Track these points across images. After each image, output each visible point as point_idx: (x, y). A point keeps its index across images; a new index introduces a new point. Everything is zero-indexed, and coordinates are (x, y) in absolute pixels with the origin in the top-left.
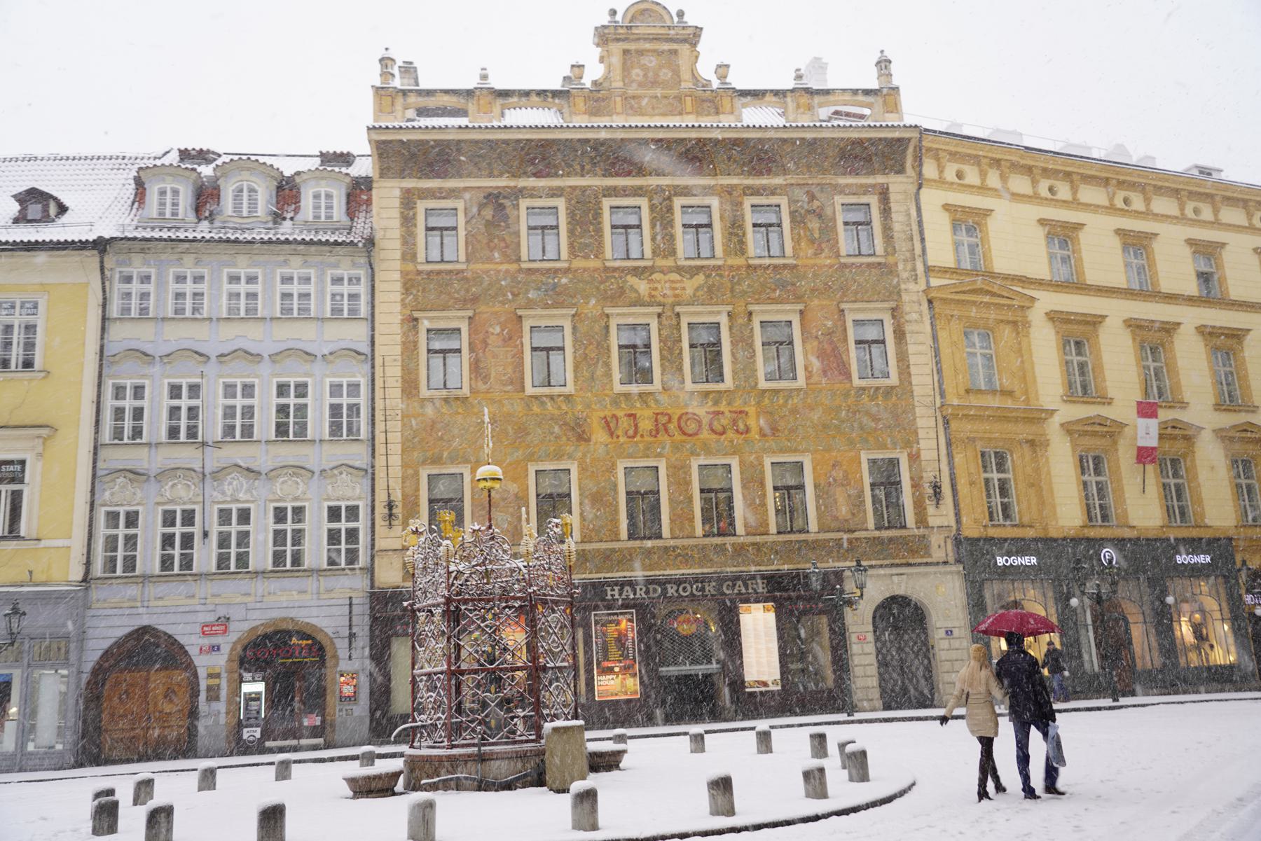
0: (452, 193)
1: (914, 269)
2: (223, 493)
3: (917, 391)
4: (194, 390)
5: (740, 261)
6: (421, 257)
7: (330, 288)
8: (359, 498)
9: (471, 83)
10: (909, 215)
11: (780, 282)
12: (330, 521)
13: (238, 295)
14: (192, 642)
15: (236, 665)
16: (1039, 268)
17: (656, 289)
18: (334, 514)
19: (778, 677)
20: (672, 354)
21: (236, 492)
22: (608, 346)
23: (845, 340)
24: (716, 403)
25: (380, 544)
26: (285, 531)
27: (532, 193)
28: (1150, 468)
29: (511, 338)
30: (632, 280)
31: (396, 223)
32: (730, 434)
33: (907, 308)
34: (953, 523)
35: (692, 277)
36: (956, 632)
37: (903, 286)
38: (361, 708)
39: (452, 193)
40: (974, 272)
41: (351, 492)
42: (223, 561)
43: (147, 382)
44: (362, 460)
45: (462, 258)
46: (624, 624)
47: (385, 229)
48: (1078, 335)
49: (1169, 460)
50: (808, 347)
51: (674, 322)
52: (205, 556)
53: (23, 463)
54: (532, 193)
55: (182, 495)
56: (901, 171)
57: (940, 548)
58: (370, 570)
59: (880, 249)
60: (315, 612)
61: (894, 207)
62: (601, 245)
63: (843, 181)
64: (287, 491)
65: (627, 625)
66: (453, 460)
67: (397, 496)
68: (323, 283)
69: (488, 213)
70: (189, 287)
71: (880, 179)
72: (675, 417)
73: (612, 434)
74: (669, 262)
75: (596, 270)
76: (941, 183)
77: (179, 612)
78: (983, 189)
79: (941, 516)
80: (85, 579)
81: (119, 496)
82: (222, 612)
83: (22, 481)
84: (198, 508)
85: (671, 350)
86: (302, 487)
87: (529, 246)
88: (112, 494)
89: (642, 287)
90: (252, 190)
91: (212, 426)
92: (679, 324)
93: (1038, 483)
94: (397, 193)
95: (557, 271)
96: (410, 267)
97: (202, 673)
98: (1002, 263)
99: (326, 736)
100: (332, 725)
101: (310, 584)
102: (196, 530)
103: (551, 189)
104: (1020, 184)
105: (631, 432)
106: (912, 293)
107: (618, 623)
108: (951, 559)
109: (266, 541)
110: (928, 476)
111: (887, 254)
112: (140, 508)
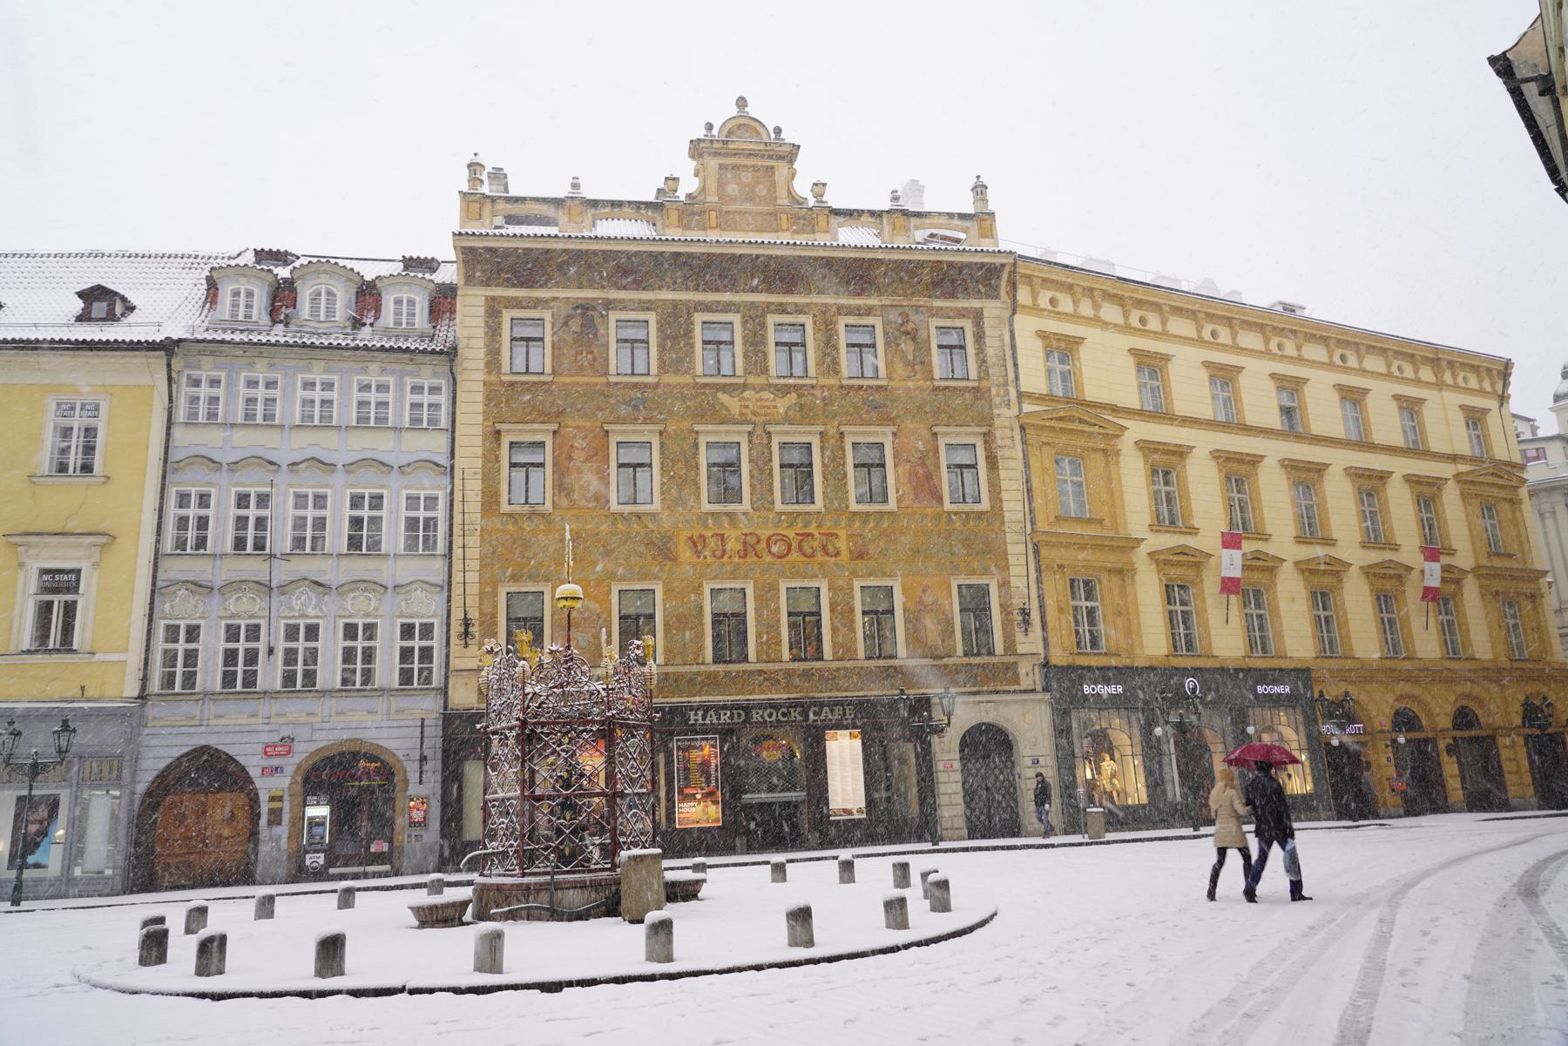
0: (537, 303)
1: (1008, 394)
2: (291, 609)
3: (1008, 516)
4: (263, 500)
5: (832, 381)
6: (506, 368)
7: (410, 398)
8: (434, 616)
9: (562, 191)
10: (1002, 341)
11: (875, 404)
12: (402, 638)
13: (313, 402)
14: (253, 764)
15: (299, 788)
16: (1129, 397)
18: (407, 631)
19: (863, 804)
21: (304, 606)
23: (938, 466)
24: (806, 525)
25: (456, 663)
26: (354, 648)
27: (622, 305)
28: (1233, 598)
29: (599, 452)
30: (723, 397)
31: (481, 332)
32: (820, 557)
33: (998, 434)
34: (1041, 651)
36: (1042, 762)
37: (996, 412)
38: (432, 834)
39: (537, 303)
40: (1068, 400)
41: (427, 608)
42: (289, 679)
43: (213, 491)
44: (440, 578)
45: (548, 370)
46: (706, 751)
47: (469, 338)
48: (1165, 465)
49: (1250, 591)
50: (900, 470)
52: (270, 674)
53: (78, 572)
54: (622, 305)
55: (246, 608)
56: (997, 297)
57: (1029, 675)
58: (444, 691)
59: (973, 374)
60: (385, 733)
61: (988, 332)
62: (692, 361)
63: (938, 303)
64: (357, 608)
65: (707, 751)
66: (532, 577)
67: (474, 615)
68: (401, 392)
69: (575, 325)
70: (261, 393)
71: (976, 304)
72: (764, 538)
73: (698, 554)
74: (762, 380)
76: (1035, 309)
77: (240, 732)
78: (1074, 317)
79: (1031, 643)
80: (143, 696)
81: (181, 609)
82: (285, 732)
83: (76, 590)
84: (263, 623)
85: (761, 471)
86: (374, 603)
87: (617, 360)
88: (172, 607)
89: (731, 403)
90: (329, 293)
91: (281, 537)
93: (1126, 614)
94: (482, 301)
95: (646, 386)
96: (493, 378)
97: (264, 797)
98: (1092, 393)
99: (392, 862)
100: (401, 850)
101: (380, 704)
102: (261, 646)
103: (640, 301)
104: (1111, 313)
105: (718, 553)
106: (1005, 417)
107: (702, 749)
108: (1039, 688)
109: (335, 658)
110: (1017, 602)
111: (980, 379)
112: (202, 622)
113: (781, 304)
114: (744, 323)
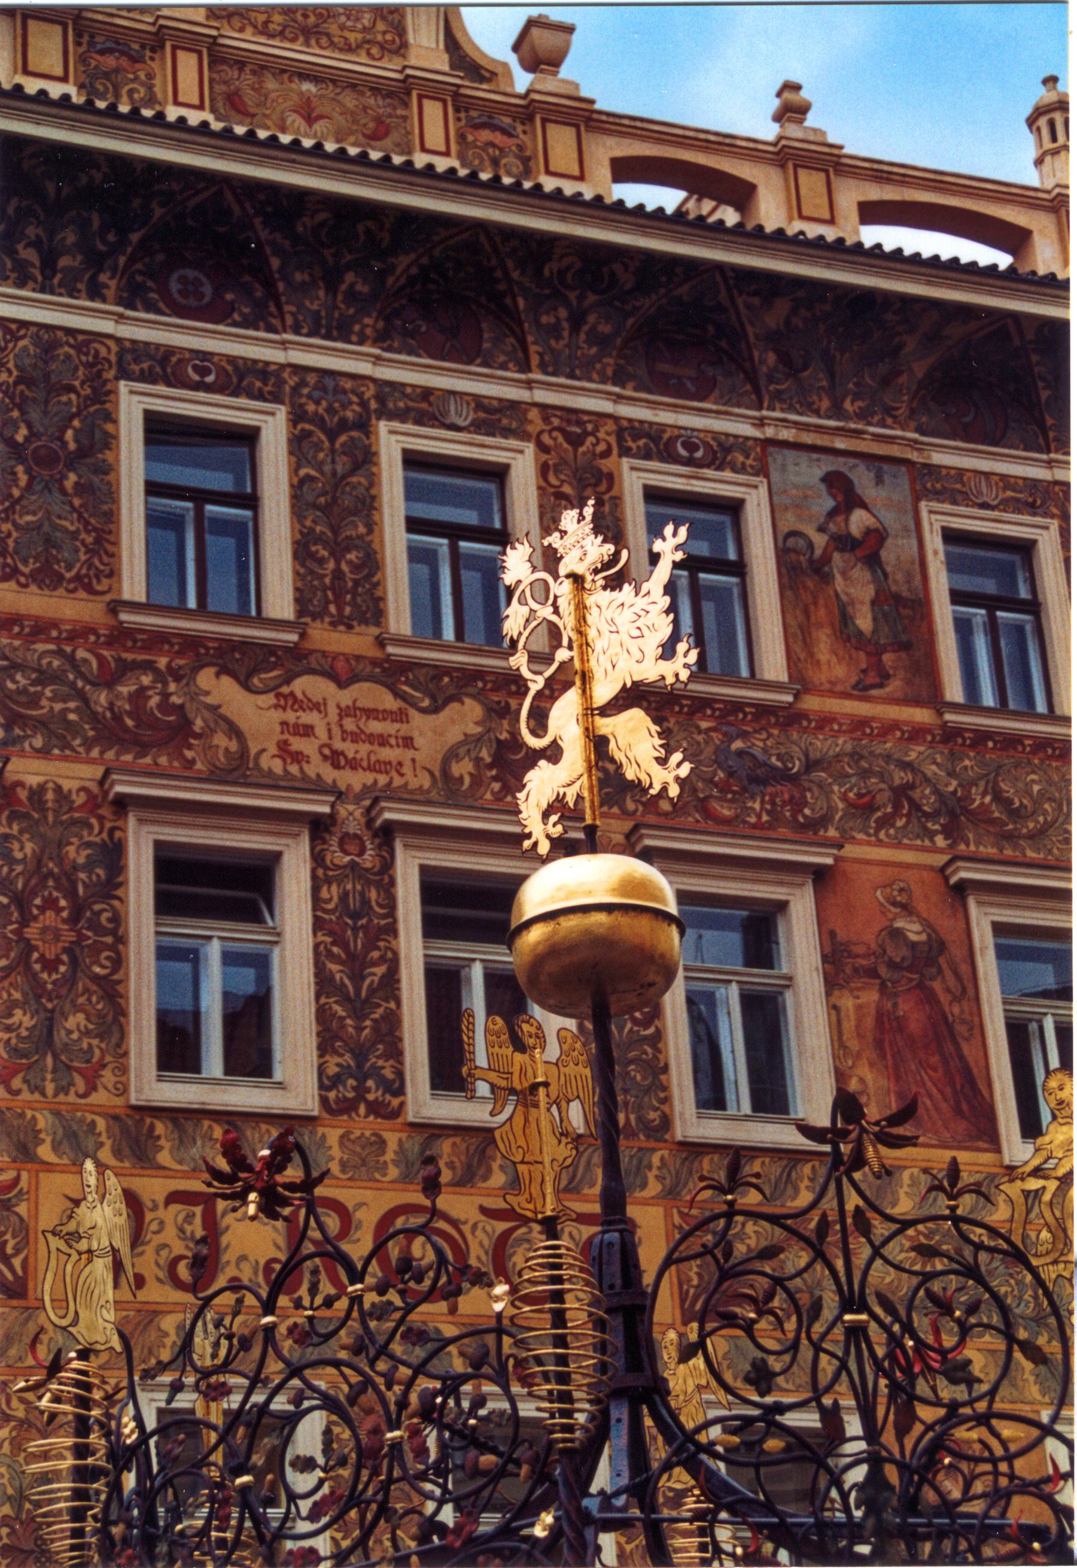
17: (307, 731)
20: (358, 978)
22: (118, 919)
30: (220, 689)
35: (435, 710)
51: (369, 859)
63: (948, 456)
74: (356, 642)
75: (80, 633)
85: (357, 965)
89: (253, 712)
92: (387, 865)
113: (427, 393)
114: (298, 444)
